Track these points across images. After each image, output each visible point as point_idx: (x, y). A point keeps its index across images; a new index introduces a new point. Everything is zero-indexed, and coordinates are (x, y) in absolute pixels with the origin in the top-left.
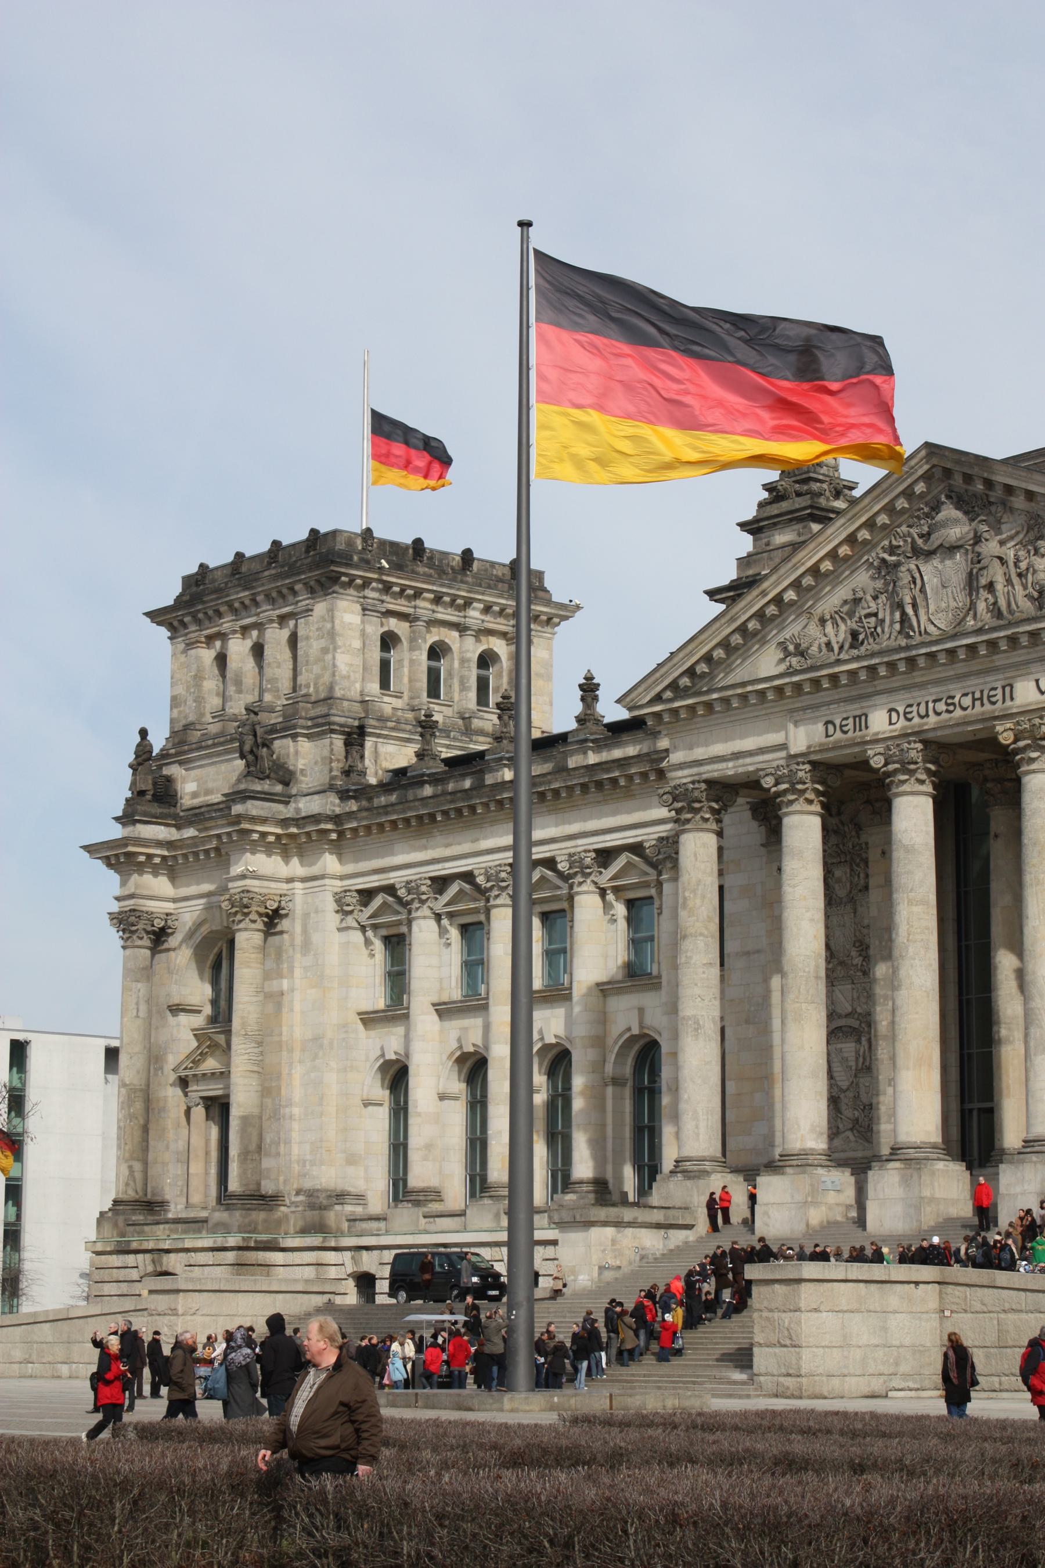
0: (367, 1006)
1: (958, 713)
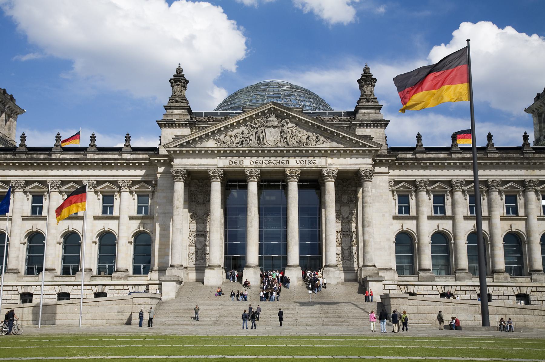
0: (25, 214)
1: (272, 165)
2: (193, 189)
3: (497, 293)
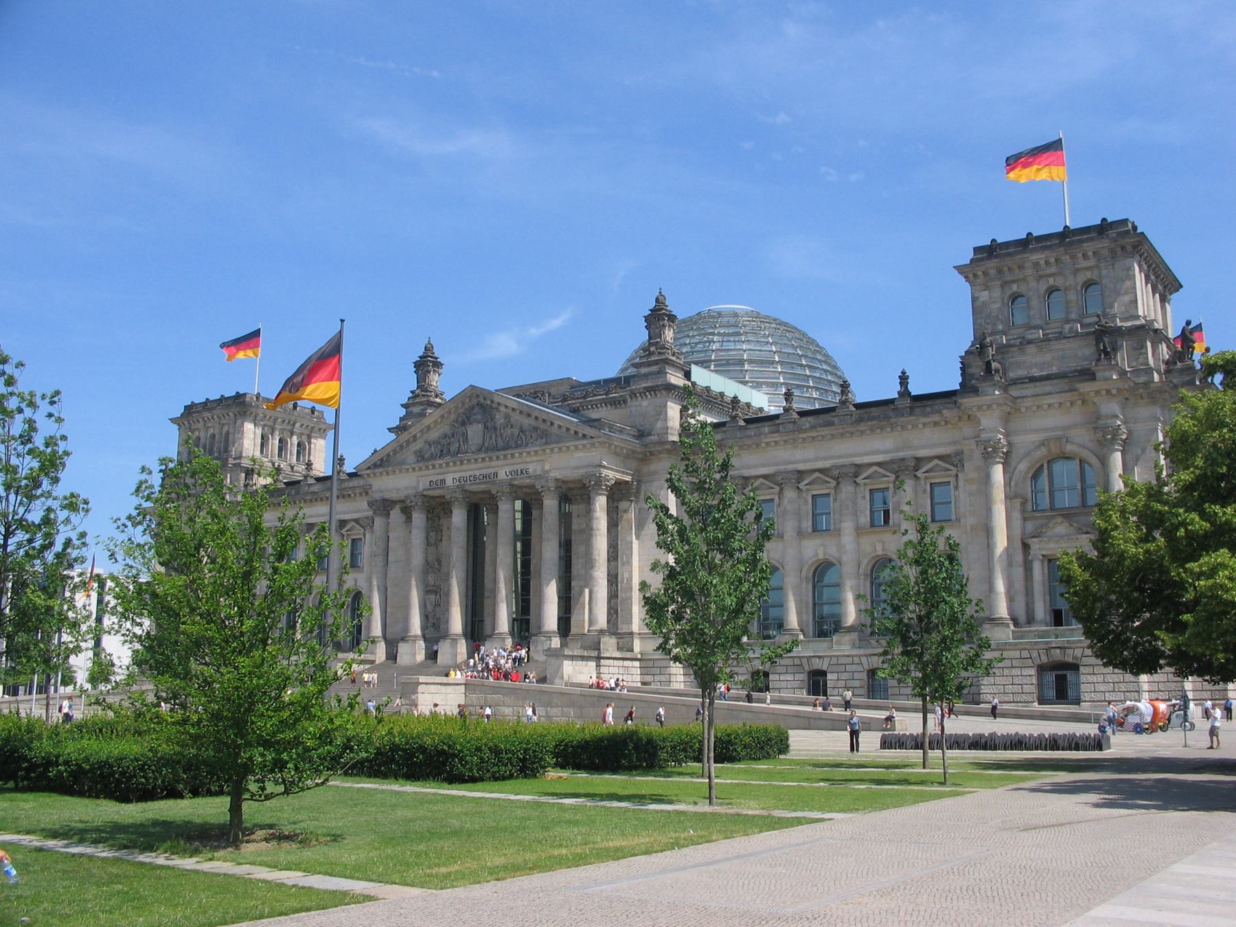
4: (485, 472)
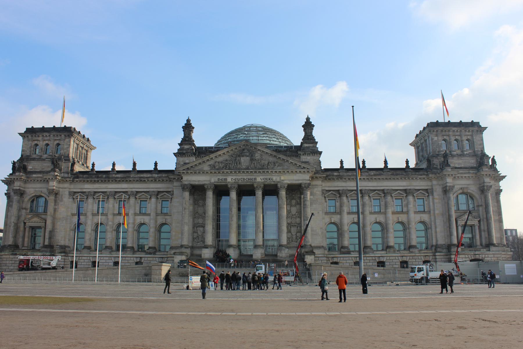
2: (196, 197)
3: (389, 261)
4: (249, 177)
